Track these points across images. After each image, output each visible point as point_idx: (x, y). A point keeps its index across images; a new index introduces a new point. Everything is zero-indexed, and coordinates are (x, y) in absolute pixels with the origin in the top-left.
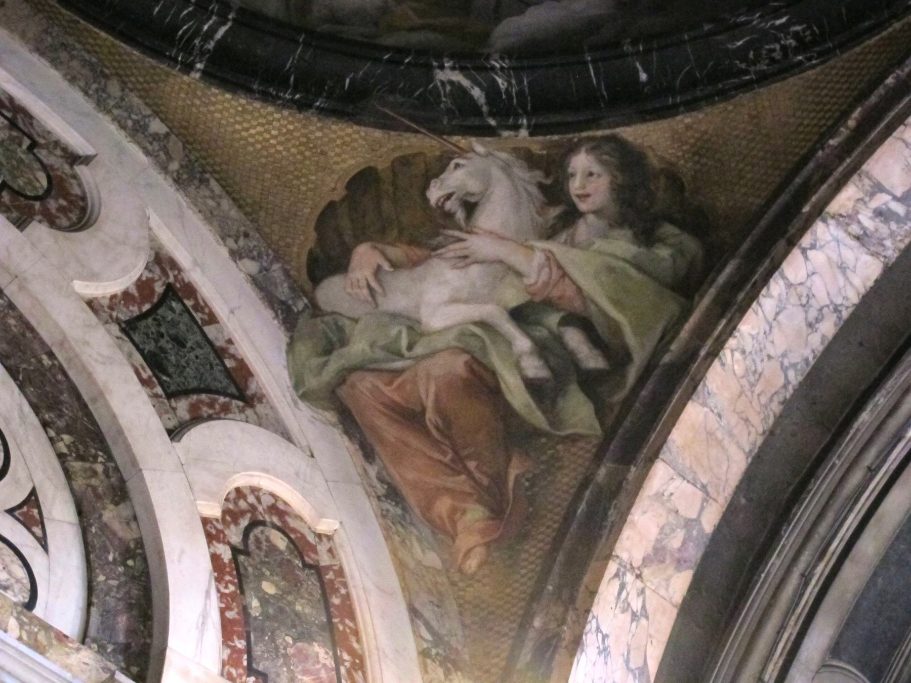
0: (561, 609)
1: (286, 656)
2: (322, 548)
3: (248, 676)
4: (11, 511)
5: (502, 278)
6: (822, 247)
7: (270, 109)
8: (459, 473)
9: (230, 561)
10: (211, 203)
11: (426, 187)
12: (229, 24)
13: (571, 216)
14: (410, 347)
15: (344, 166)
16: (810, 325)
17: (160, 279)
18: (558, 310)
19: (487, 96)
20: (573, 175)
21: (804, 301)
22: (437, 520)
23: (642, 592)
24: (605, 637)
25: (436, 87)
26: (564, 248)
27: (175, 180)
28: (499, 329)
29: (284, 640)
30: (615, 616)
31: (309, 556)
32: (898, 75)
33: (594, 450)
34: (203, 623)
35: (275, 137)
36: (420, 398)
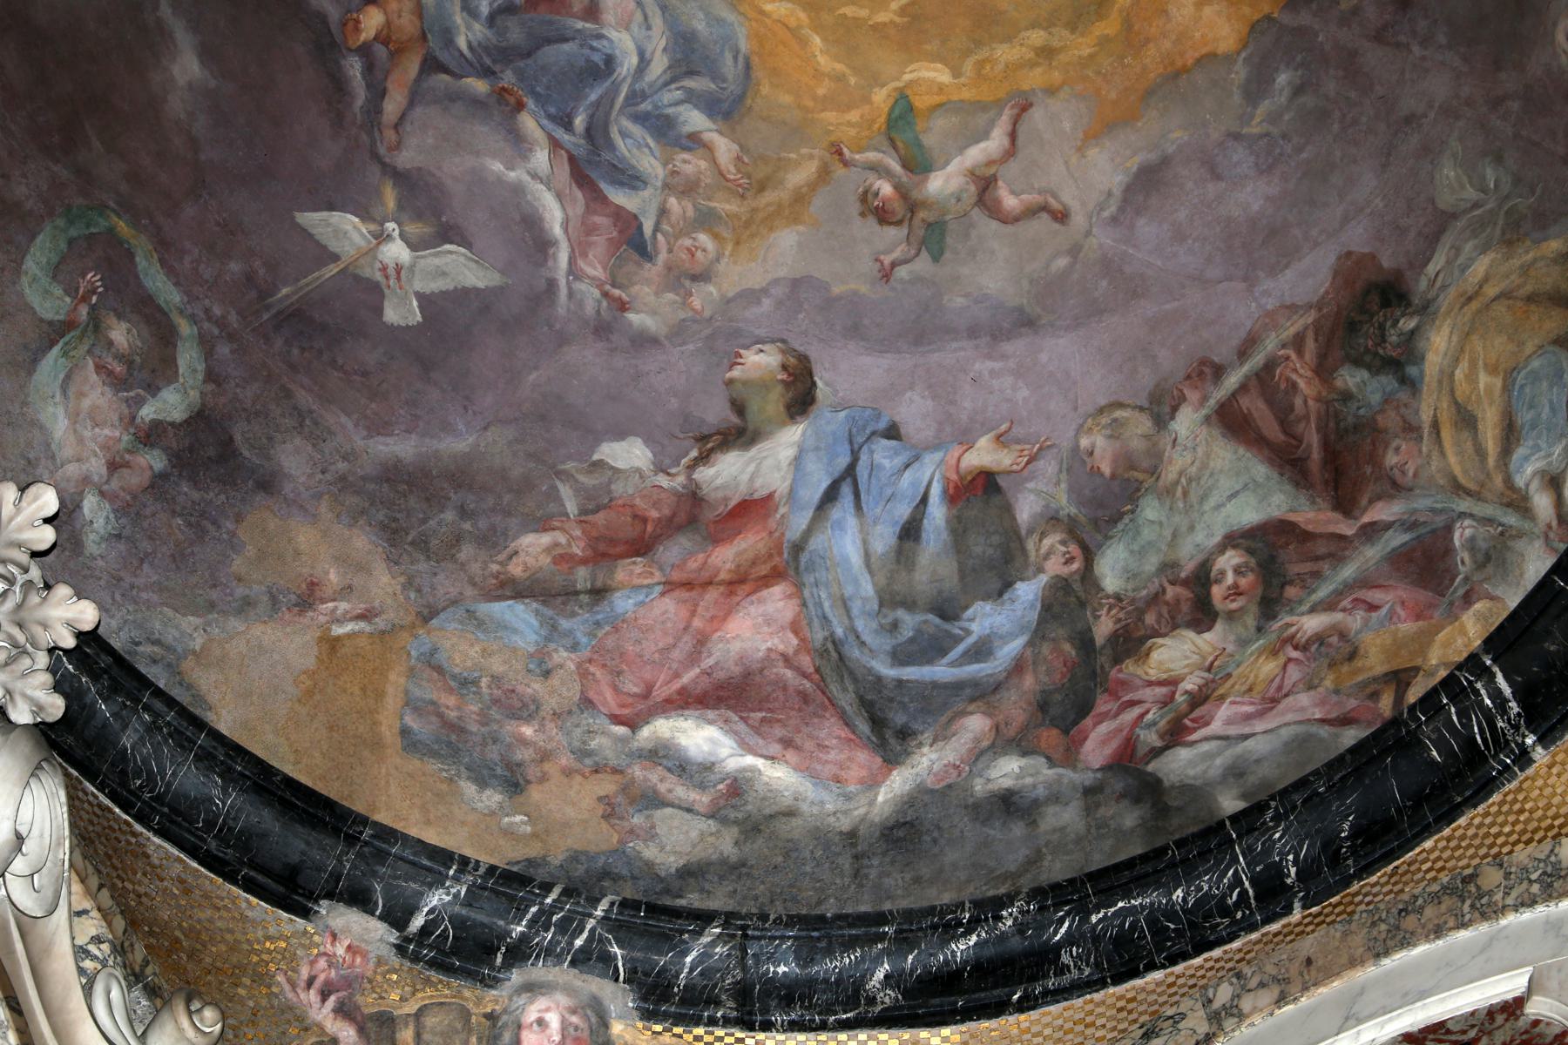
12: (1496, 669)
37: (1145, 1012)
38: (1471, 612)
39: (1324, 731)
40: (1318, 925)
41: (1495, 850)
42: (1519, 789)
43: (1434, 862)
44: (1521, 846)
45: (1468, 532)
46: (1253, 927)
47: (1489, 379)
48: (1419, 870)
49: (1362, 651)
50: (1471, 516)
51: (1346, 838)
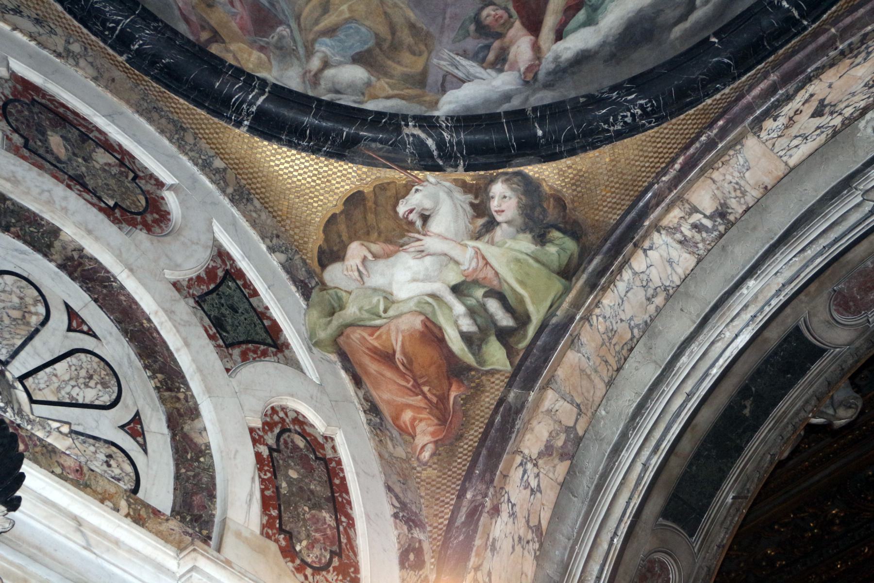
0: (484, 487)
1: (304, 520)
2: (328, 446)
3: (279, 534)
4: (122, 427)
5: (446, 265)
6: (656, 248)
7: (294, 152)
8: (417, 395)
9: (268, 456)
10: (254, 215)
11: (396, 204)
13: (492, 224)
14: (385, 311)
15: (341, 189)
16: (648, 299)
17: (221, 267)
18: (484, 287)
19: (437, 145)
20: (493, 197)
21: (645, 283)
22: (403, 425)
23: (538, 475)
24: (513, 505)
25: (403, 138)
26: (487, 246)
27: (230, 200)
28: (444, 299)
29: (303, 509)
30: (520, 491)
31: (319, 452)
32: (709, 135)
33: (506, 380)
34: (250, 500)
35: (296, 170)
36: (392, 345)
37: (43, 12)
38: (259, 53)
39: (177, 12)
40: (124, 71)
41: (197, 131)
42: (225, 128)
43: (177, 108)
44: (205, 141)
45: (284, 33)
46: (105, 42)
47: (346, 10)
48: (170, 103)
49: (214, 9)
50: (291, 31)
51: (163, 63)
